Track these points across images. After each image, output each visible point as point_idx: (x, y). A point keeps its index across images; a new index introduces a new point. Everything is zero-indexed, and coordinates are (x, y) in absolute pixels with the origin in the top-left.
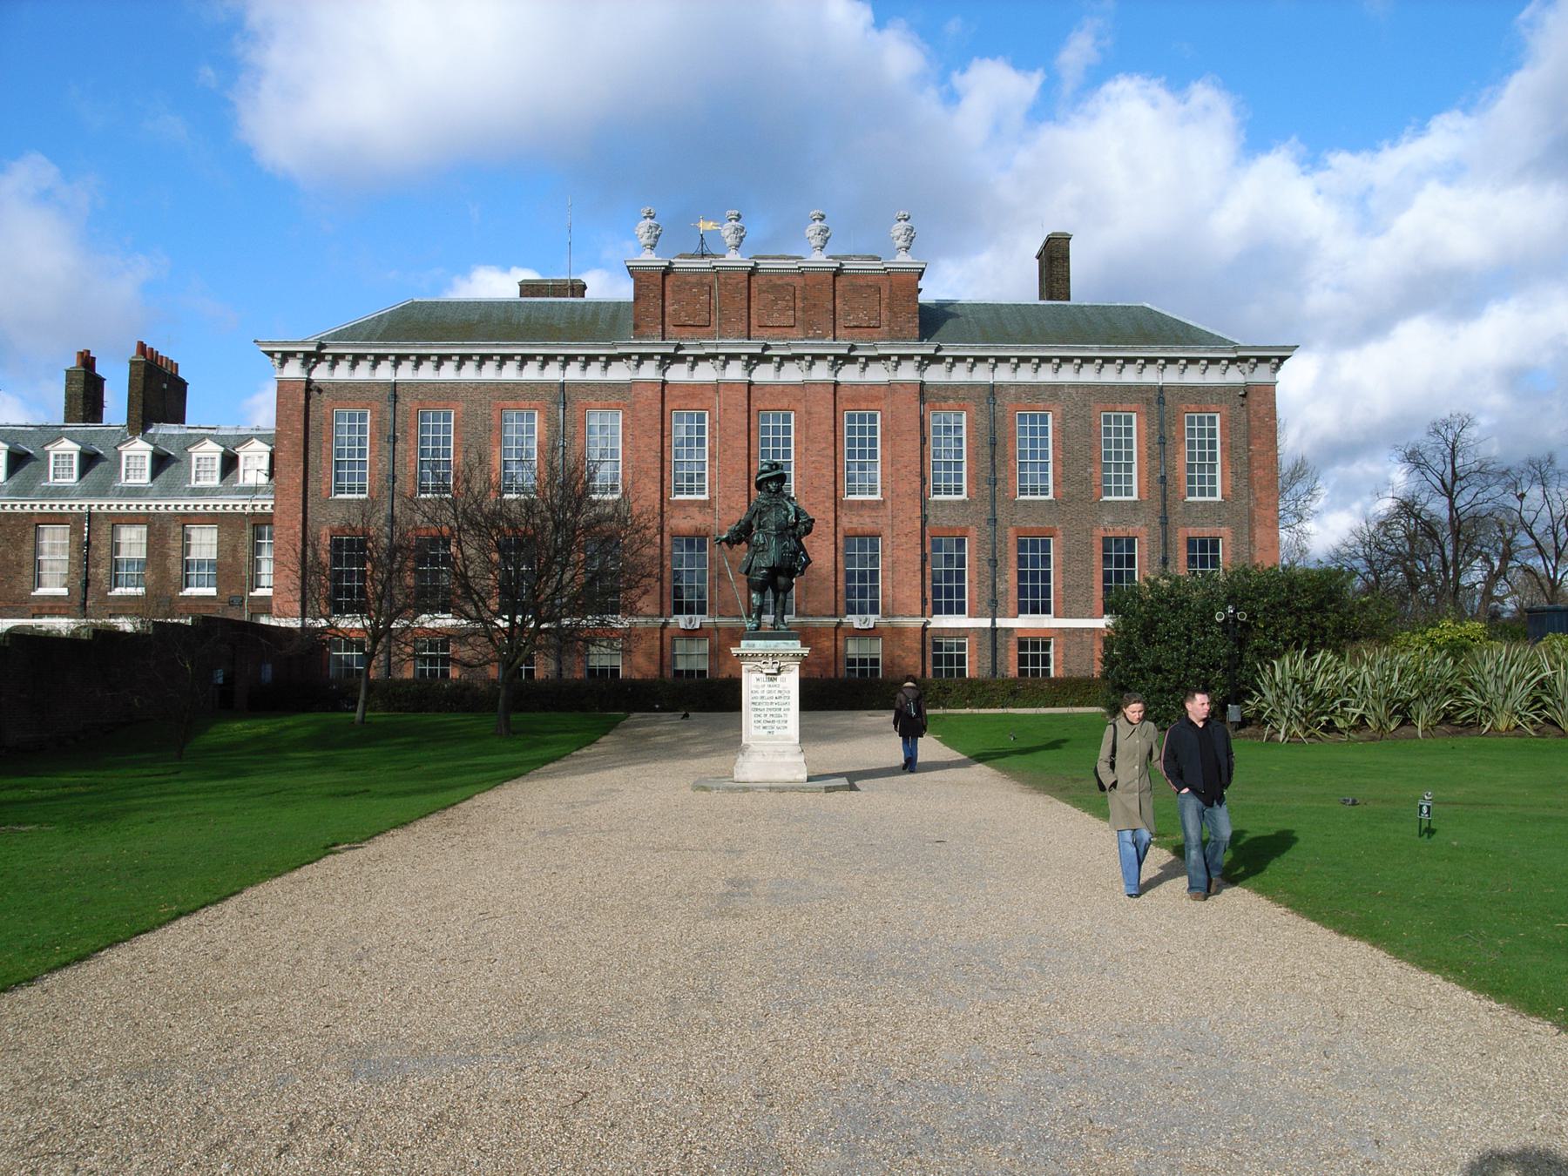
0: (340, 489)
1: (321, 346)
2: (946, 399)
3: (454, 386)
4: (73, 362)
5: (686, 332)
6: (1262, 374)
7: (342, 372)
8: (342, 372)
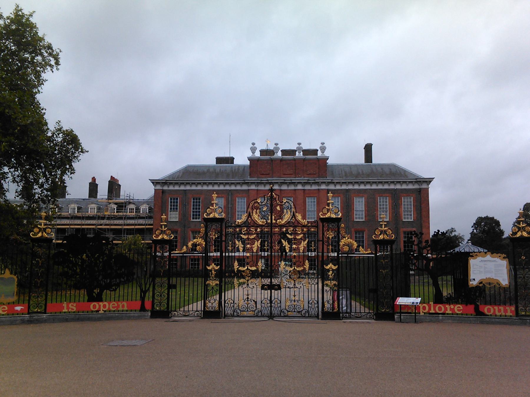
3: (201, 190)
5: (263, 176)
6: (424, 186)
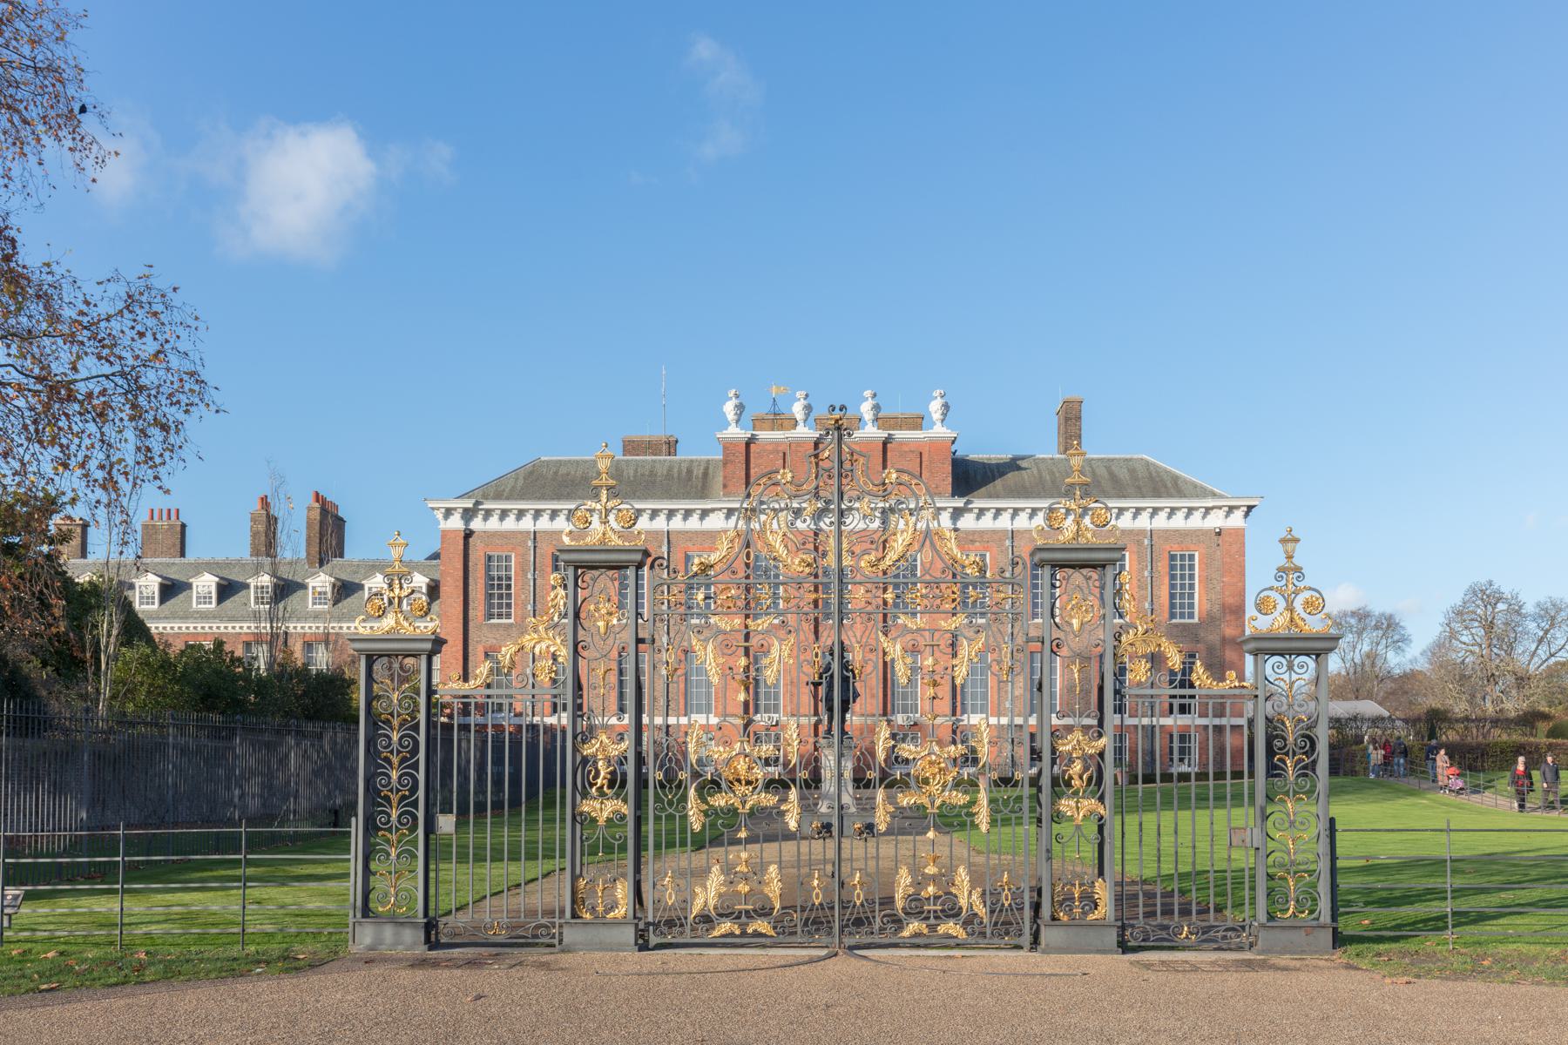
0: (491, 616)
1: (477, 503)
2: (973, 541)
4: (257, 506)
7: (493, 524)
8: (493, 524)
